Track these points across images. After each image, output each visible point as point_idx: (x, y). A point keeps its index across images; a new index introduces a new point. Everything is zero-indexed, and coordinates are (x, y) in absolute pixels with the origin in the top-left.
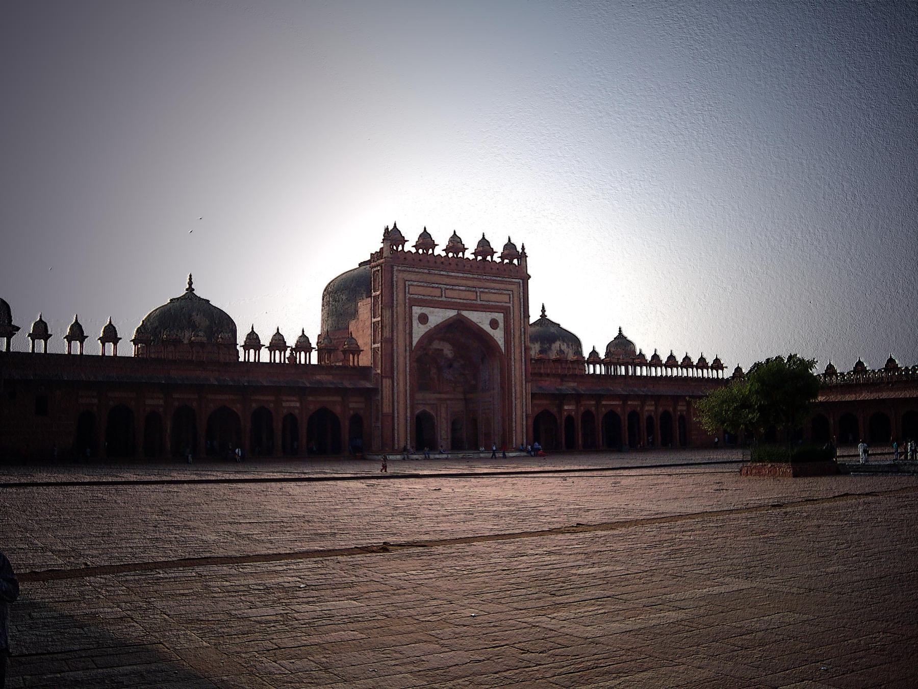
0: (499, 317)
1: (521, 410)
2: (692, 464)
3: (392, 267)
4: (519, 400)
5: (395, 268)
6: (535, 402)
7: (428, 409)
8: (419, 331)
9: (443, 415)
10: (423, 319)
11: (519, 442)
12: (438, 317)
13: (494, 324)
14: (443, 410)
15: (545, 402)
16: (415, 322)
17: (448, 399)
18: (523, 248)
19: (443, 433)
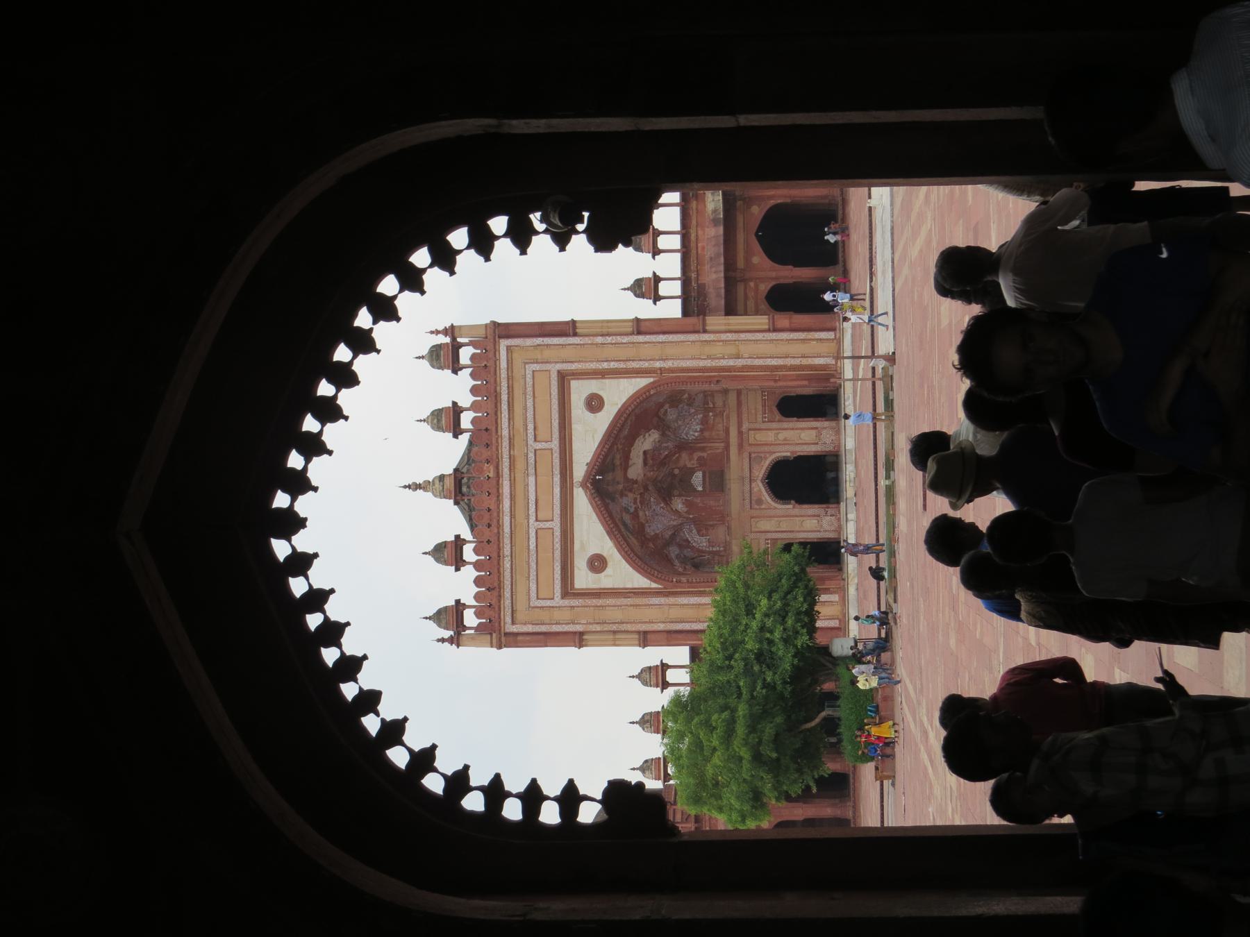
0: (580, 390)
1: (759, 346)
2: (871, 253)
3: (506, 634)
4: (744, 350)
5: (511, 629)
6: (740, 307)
7: (761, 471)
8: (622, 574)
9: (769, 437)
10: (598, 563)
11: (824, 348)
12: (591, 533)
13: (594, 404)
14: (761, 437)
15: (741, 237)
16: (606, 580)
17: (740, 425)
18: (437, 332)
19: (803, 437)
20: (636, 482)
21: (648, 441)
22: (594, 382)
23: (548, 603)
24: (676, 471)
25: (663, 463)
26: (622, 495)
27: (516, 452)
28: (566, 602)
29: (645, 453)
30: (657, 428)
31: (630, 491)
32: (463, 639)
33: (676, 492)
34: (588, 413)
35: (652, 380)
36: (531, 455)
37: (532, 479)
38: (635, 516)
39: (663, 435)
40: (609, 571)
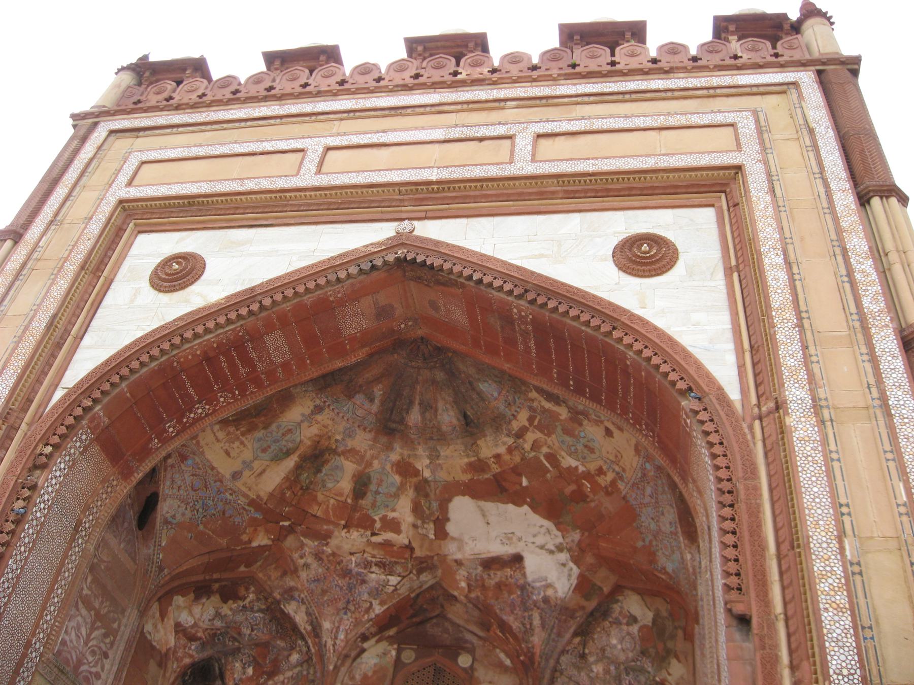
20: (442, 533)
21: (550, 568)
22: (714, 254)
23: (123, 178)
24: (464, 661)
25: (487, 618)
26: (405, 469)
27: (511, 114)
28: (106, 208)
29: (518, 559)
30: (584, 586)
31: (417, 509)
32: (128, 78)
33: (409, 656)
34: (615, 241)
35: (734, 394)
36: (501, 130)
37: (438, 134)
38: (354, 515)
39: (565, 611)
40: (150, 295)
